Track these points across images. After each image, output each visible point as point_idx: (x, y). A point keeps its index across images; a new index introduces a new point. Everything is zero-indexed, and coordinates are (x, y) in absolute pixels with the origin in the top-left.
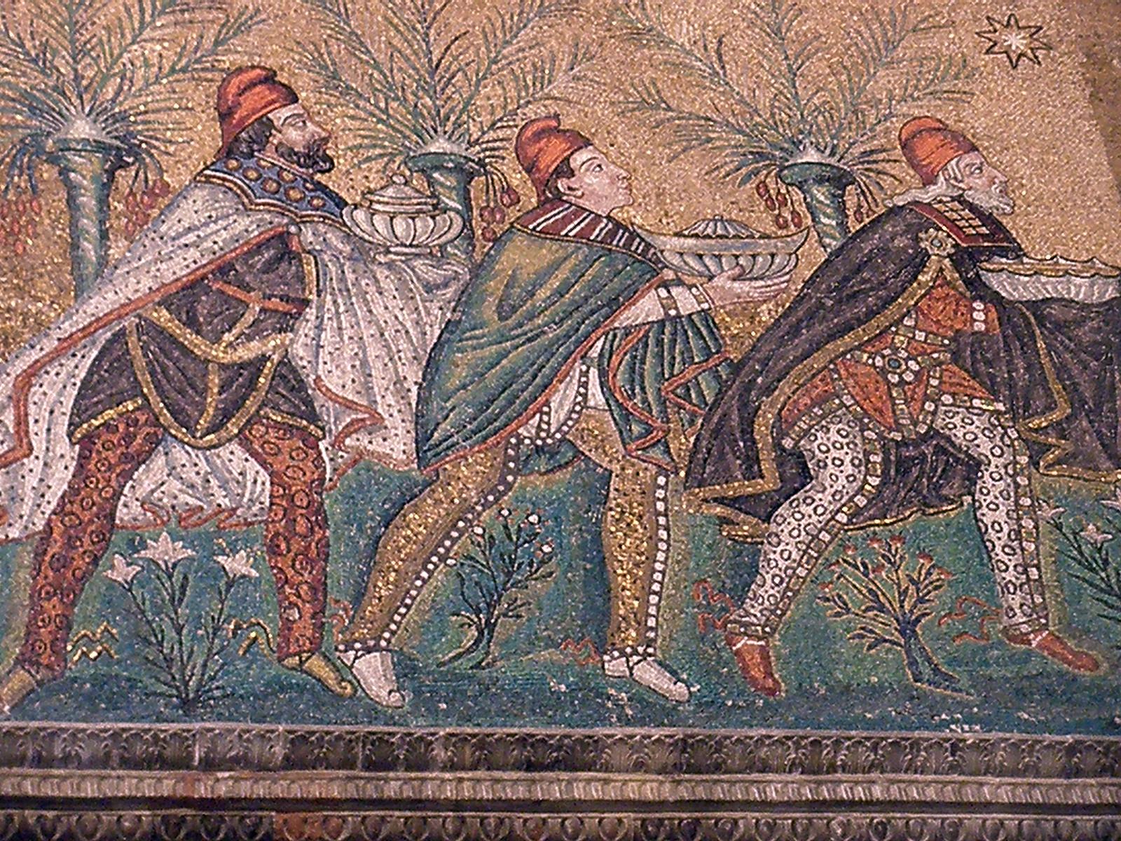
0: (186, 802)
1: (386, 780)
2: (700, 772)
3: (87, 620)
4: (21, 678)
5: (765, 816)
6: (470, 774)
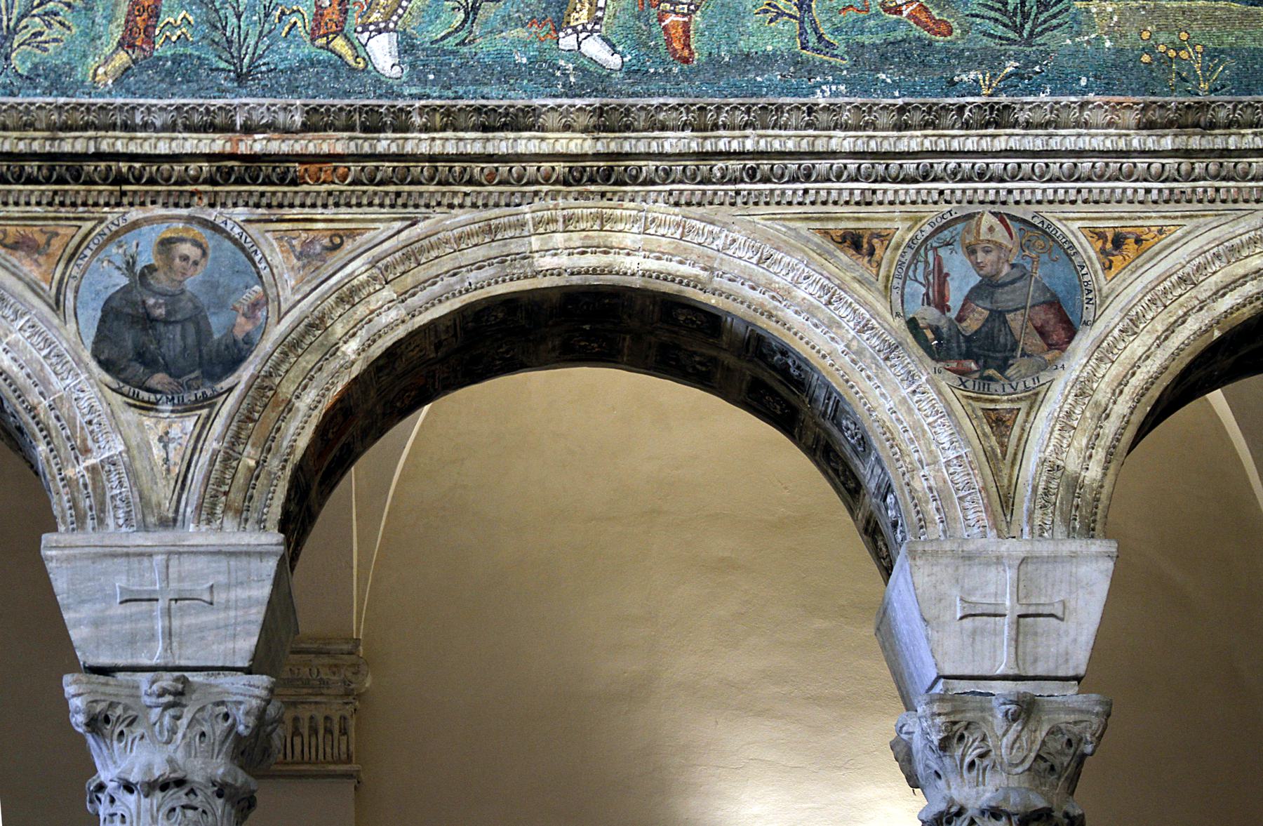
0: (233, 156)
1: (379, 140)
2: (614, 131)
3: (171, 10)
4: (122, 58)
5: (664, 164)
6: (441, 135)
